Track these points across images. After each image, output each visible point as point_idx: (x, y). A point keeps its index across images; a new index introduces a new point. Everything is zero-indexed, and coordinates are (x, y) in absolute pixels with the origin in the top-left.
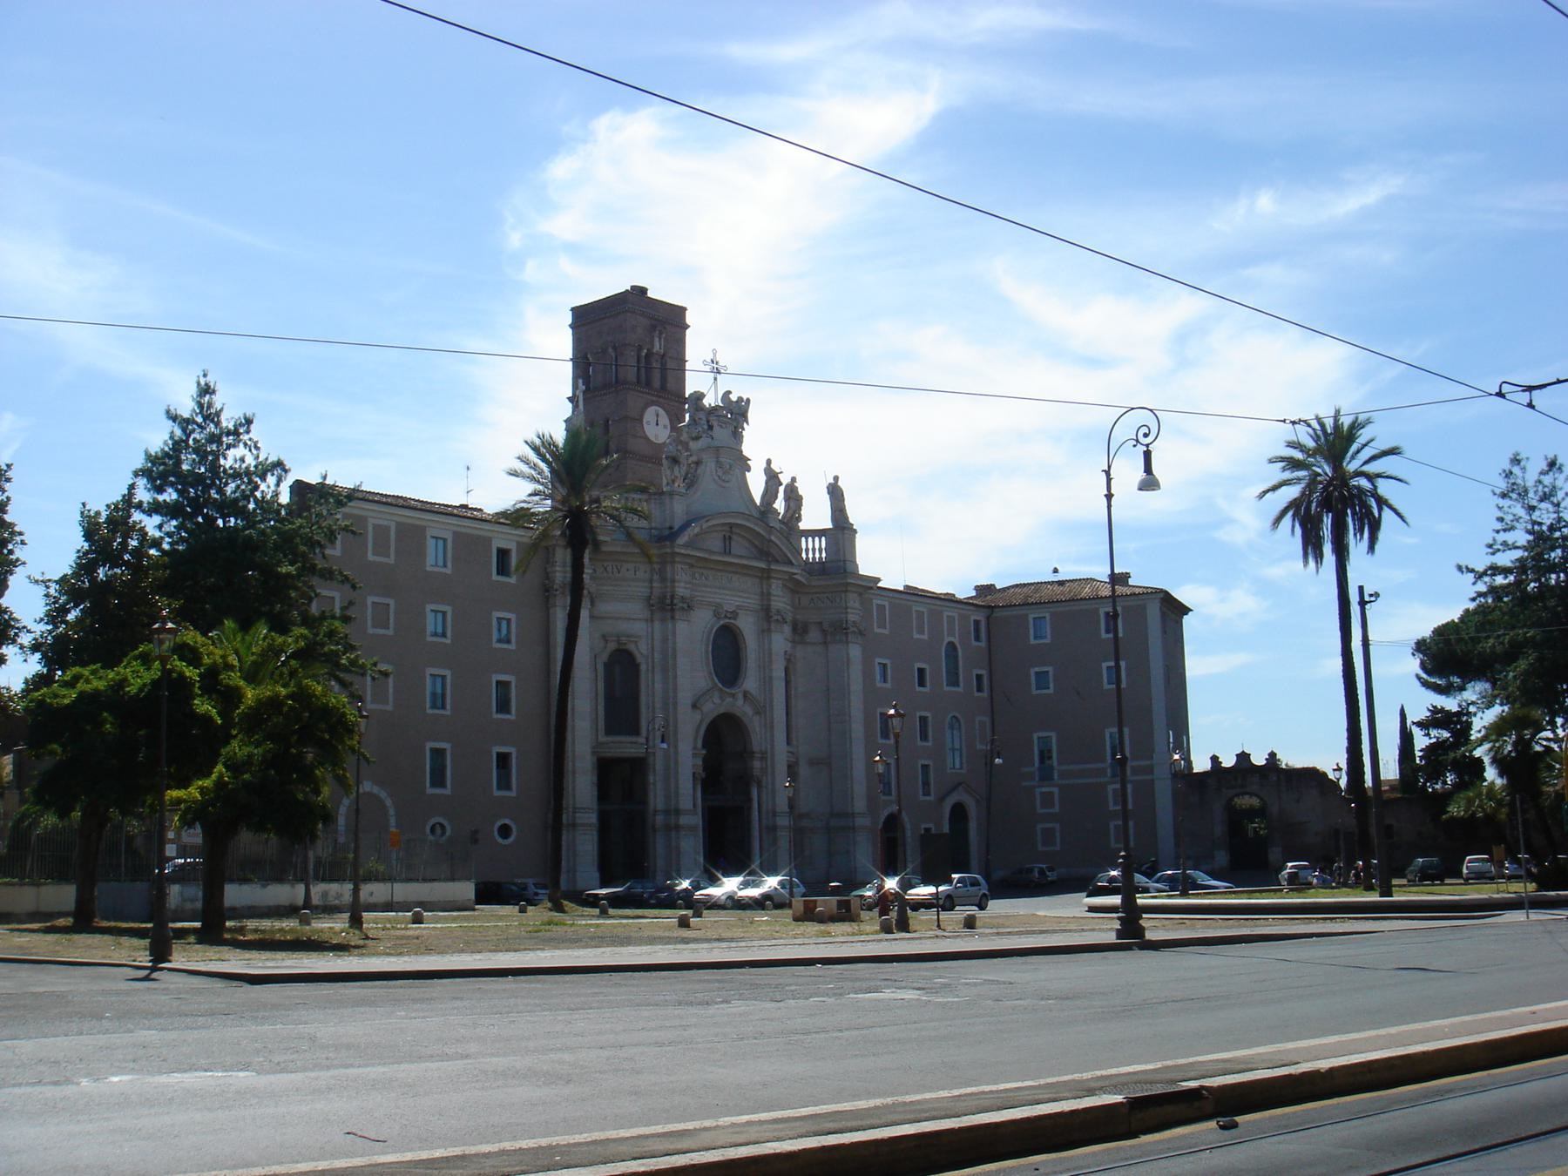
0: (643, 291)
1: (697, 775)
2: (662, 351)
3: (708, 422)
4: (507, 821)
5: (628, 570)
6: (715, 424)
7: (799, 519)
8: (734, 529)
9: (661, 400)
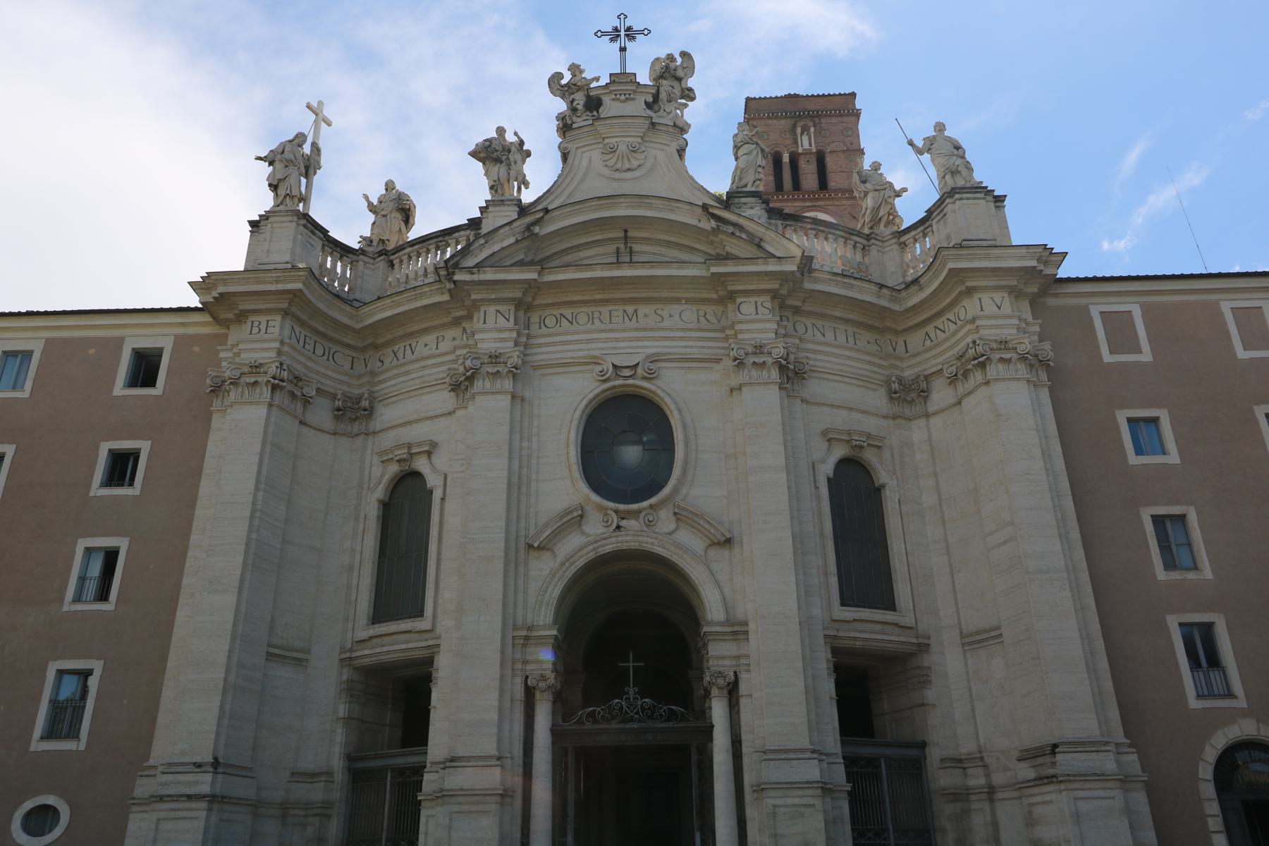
1: (529, 683)
4: (50, 800)
5: (426, 345)
6: (606, 100)
8: (630, 234)
9: (818, 203)
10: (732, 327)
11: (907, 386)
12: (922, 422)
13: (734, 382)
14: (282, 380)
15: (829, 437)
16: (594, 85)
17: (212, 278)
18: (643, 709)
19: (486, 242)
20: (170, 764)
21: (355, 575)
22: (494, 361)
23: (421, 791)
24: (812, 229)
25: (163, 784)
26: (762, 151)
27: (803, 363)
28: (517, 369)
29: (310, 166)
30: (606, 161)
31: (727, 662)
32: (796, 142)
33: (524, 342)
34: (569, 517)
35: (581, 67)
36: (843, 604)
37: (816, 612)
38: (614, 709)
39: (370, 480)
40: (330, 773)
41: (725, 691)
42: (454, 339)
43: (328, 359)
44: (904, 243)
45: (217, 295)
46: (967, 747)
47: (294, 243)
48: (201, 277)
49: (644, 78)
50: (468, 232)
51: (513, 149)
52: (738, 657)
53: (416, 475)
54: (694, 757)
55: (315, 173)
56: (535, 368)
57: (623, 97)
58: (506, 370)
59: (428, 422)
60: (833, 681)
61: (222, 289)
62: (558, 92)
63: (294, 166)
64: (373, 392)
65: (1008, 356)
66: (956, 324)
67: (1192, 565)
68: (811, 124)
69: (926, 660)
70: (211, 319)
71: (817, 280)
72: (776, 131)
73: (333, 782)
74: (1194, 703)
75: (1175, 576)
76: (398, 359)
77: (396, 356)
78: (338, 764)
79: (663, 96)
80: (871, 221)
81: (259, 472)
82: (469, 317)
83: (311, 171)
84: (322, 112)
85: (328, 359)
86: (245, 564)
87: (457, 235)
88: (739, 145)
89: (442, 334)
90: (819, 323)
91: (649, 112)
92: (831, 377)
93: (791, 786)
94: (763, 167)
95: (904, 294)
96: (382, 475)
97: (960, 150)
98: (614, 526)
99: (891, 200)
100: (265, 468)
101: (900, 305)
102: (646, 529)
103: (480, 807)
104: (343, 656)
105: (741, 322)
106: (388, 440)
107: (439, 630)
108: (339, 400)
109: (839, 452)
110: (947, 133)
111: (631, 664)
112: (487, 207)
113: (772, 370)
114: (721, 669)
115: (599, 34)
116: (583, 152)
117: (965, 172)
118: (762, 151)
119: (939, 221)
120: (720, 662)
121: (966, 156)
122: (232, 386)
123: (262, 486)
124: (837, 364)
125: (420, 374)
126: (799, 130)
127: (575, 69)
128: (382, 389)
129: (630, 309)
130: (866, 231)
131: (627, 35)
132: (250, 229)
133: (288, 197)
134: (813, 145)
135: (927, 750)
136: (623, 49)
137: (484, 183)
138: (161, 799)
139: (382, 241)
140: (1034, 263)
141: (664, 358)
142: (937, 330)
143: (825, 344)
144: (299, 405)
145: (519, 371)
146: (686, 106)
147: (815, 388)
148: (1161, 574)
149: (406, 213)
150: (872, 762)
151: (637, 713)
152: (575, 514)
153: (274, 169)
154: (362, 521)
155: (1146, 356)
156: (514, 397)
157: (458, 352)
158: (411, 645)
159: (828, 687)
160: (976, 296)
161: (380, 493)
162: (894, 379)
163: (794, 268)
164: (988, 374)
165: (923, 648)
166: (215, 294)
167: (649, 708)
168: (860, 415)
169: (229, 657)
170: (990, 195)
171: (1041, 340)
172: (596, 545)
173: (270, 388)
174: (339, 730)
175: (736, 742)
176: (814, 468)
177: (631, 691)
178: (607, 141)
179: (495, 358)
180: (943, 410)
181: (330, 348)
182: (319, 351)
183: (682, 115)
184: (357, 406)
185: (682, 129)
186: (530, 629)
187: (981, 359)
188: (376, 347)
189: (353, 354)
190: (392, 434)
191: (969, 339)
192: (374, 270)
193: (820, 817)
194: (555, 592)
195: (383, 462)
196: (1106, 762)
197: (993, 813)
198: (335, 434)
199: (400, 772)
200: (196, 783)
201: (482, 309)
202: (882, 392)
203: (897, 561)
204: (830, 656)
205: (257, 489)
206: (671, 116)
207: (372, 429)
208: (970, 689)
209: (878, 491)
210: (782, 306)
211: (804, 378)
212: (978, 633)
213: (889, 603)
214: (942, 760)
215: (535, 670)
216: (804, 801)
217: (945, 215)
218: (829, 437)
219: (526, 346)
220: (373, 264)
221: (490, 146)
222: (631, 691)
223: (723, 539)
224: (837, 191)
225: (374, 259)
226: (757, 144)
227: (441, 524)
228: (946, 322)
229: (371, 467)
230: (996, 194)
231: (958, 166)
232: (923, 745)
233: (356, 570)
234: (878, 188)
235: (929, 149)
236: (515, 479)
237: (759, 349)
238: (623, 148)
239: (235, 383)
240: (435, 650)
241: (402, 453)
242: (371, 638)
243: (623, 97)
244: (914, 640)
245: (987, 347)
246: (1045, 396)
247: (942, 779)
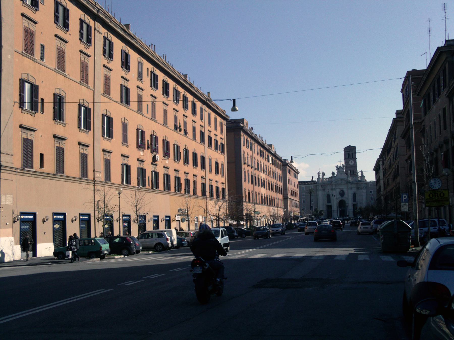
0: (350, 145)
78: (326, 210)
109: (354, 193)
127: (337, 166)
161: (327, 195)
213: (356, 201)
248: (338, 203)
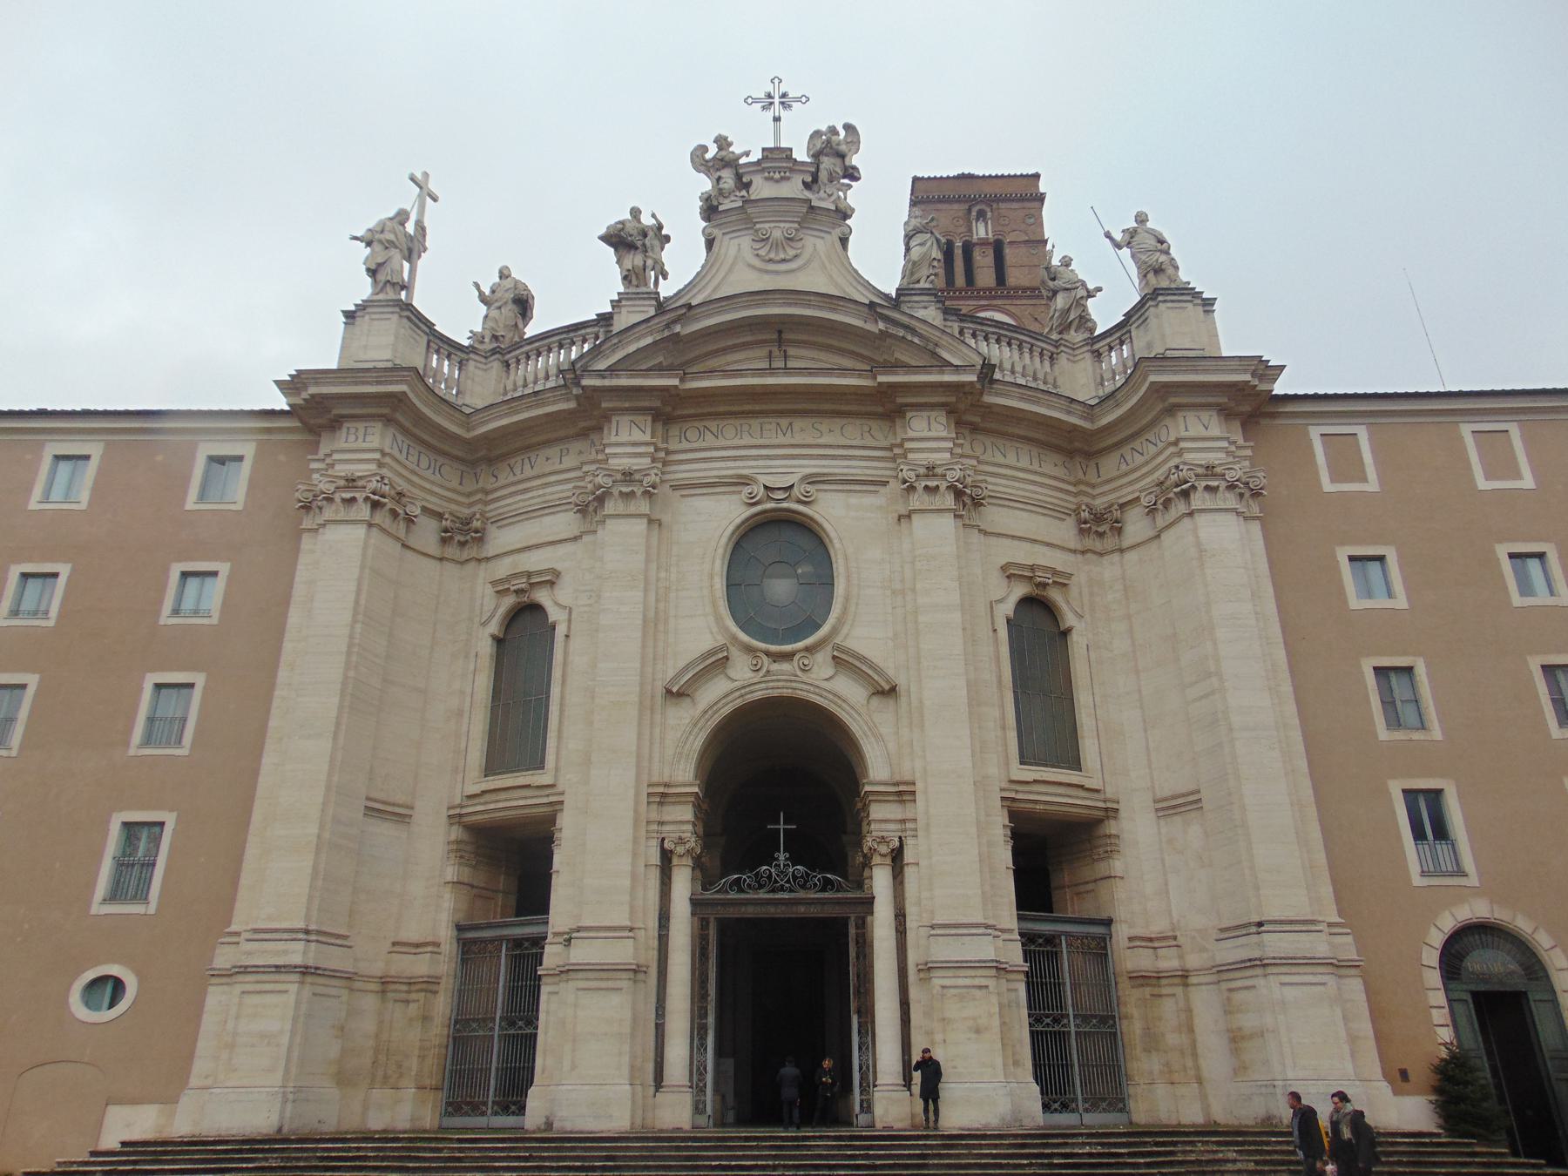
1: (666, 845)
2: (990, 235)
3: (739, 177)
4: (114, 970)
5: (547, 459)
7: (1084, 321)
8: (785, 336)
10: (901, 445)
11: (1098, 516)
12: (1116, 557)
13: (904, 512)
14: (383, 496)
15: (1010, 573)
16: (743, 161)
17: (303, 376)
18: (795, 877)
19: (620, 342)
20: (256, 931)
21: (466, 720)
22: (628, 478)
23: (541, 965)
24: (993, 333)
25: (249, 953)
26: (938, 240)
27: (982, 489)
28: (654, 488)
29: (413, 248)
30: (755, 249)
31: (892, 826)
32: (970, 230)
33: (663, 459)
34: (713, 659)
35: (729, 140)
36: (1022, 763)
37: (993, 770)
38: (762, 877)
39: (481, 613)
40: (437, 945)
41: (888, 860)
42: (581, 452)
43: (434, 473)
44: (1098, 351)
45: (308, 397)
46: (1158, 927)
47: (396, 337)
48: (290, 375)
49: (801, 155)
50: (596, 329)
51: (651, 234)
52: (903, 821)
53: (536, 608)
54: (852, 931)
55: (419, 257)
56: (675, 488)
57: (777, 176)
58: (642, 490)
59: (550, 549)
60: (1010, 848)
61: (313, 390)
62: (702, 168)
63: (396, 247)
64: (486, 512)
65: (1215, 484)
66: (1156, 445)
67: (1419, 725)
68: (988, 209)
69: (1111, 827)
70: (299, 424)
71: (997, 395)
72: (947, 217)
73: (440, 953)
74: (1417, 880)
75: (1399, 735)
76: (514, 475)
77: (512, 469)
79: (823, 175)
80: (1060, 324)
81: (357, 602)
82: (599, 429)
83: (415, 256)
84: (427, 184)
85: (434, 473)
86: (341, 707)
87: (583, 332)
88: (912, 233)
89: (566, 446)
90: (1000, 442)
91: (808, 194)
92: (1012, 504)
93: (961, 966)
94: (939, 260)
95: (1097, 410)
96: (496, 609)
97: (1165, 245)
98: (764, 670)
99: (1083, 302)
100: (363, 597)
101: (1092, 422)
102: (799, 673)
103: (610, 984)
104: (452, 812)
105: (912, 440)
106: (503, 568)
107: (560, 788)
108: (447, 520)
109: (1020, 590)
110: (1149, 225)
111: (782, 827)
112: (619, 301)
113: (947, 496)
114: (884, 834)
115: (750, 101)
116: (731, 239)
117: (1170, 271)
118: (938, 240)
119: (1137, 328)
120: (884, 826)
121: (1171, 251)
122: (325, 502)
123: (360, 617)
124: (1018, 489)
125: (541, 492)
126: (974, 214)
127: (722, 142)
128: (496, 509)
129: (784, 422)
130: (1055, 336)
131: (783, 103)
132: (344, 320)
133: (388, 288)
134: (990, 232)
135: (1113, 925)
136: (777, 119)
137: (616, 273)
138: (245, 970)
139: (495, 338)
140: (1247, 377)
141: (822, 479)
142: (1134, 453)
143: (1007, 466)
144: (402, 525)
145: (656, 491)
146: (850, 187)
147: (995, 517)
148: (1383, 734)
149: (523, 305)
150: (1051, 940)
151: (788, 881)
152: (720, 656)
153: (373, 251)
154: (472, 659)
155: (1372, 485)
156: (650, 521)
157: (585, 468)
158: (529, 802)
159: (1004, 856)
160: (1180, 414)
161: (494, 627)
162: (1084, 507)
163: (974, 378)
164: (1193, 502)
165: (1111, 813)
166: (305, 395)
167: (802, 877)
168: (1045, 548)
169: (323, 811)
170: (1198, 298)
171: (1252, 466)
172: (743, 691)
173: (369, 505)
174: (447, 896)
175: (900, 916)
176: (992, 607)
177: (782, 856)
178: (758, 226)
179: (628, 476)
180: (1138, 545)
181: (436, 460)
182: (424, 462)
183: (845, 198)
184: (467, 528)
185: (844, 214)
186: (666, 785)
187: (1184, 487)
188: (491, 461)
189: (461, 468)
190: (508, 560)
191: (1172, 463)
192: (486, 370)
193: (994, 999)
194: (698, 742)
195: (497, 592)
196: (1318, 945)
197: (1187, 999)
198: (441, 559)
199: (517, 943)
200: (285, 952)
201: (614, 419)
202: (1071, 522)
203: (1083, 715)
204: (1007, 823)
205: (355, 621)
206: (833, 198)
207: (484, 555)
208: (1163, 860)
209: (1065, 633)
210: (959, 423)
211: (982, 504)
212: (1174, 797)
213: (1075, 763)
214: (1131, 939)
215: (673, 832)
216: (977, 982)
217: (1146, 319)
218: (1010, 573)
219: (665, 463)
220: (486, 364)
221: (623, 229)
222: (782, 856)
223: (887, 687)
224: (1016, 289)
225: (486, 358)
226: (932, 233)
227: (565, 664)
228: (1144, 442)
229: (483, 597)
230: (1204, 296)
231: (1162, 263)
232: (1108, 923)
233: (466, 715)
234: (1069, 286)
235: (1129, 243)
236: (651, 614)
237: (931, 470)
238: (777, 234)
239: (329, 500)
240: (558, 807)
241: (521, 583)
242: (484, 792)
243: (777, 176)
244: (1101, 805)
245: (1192, 472)
246: (1256, 527)
247: (1128, 959)
248: (685, 773)
